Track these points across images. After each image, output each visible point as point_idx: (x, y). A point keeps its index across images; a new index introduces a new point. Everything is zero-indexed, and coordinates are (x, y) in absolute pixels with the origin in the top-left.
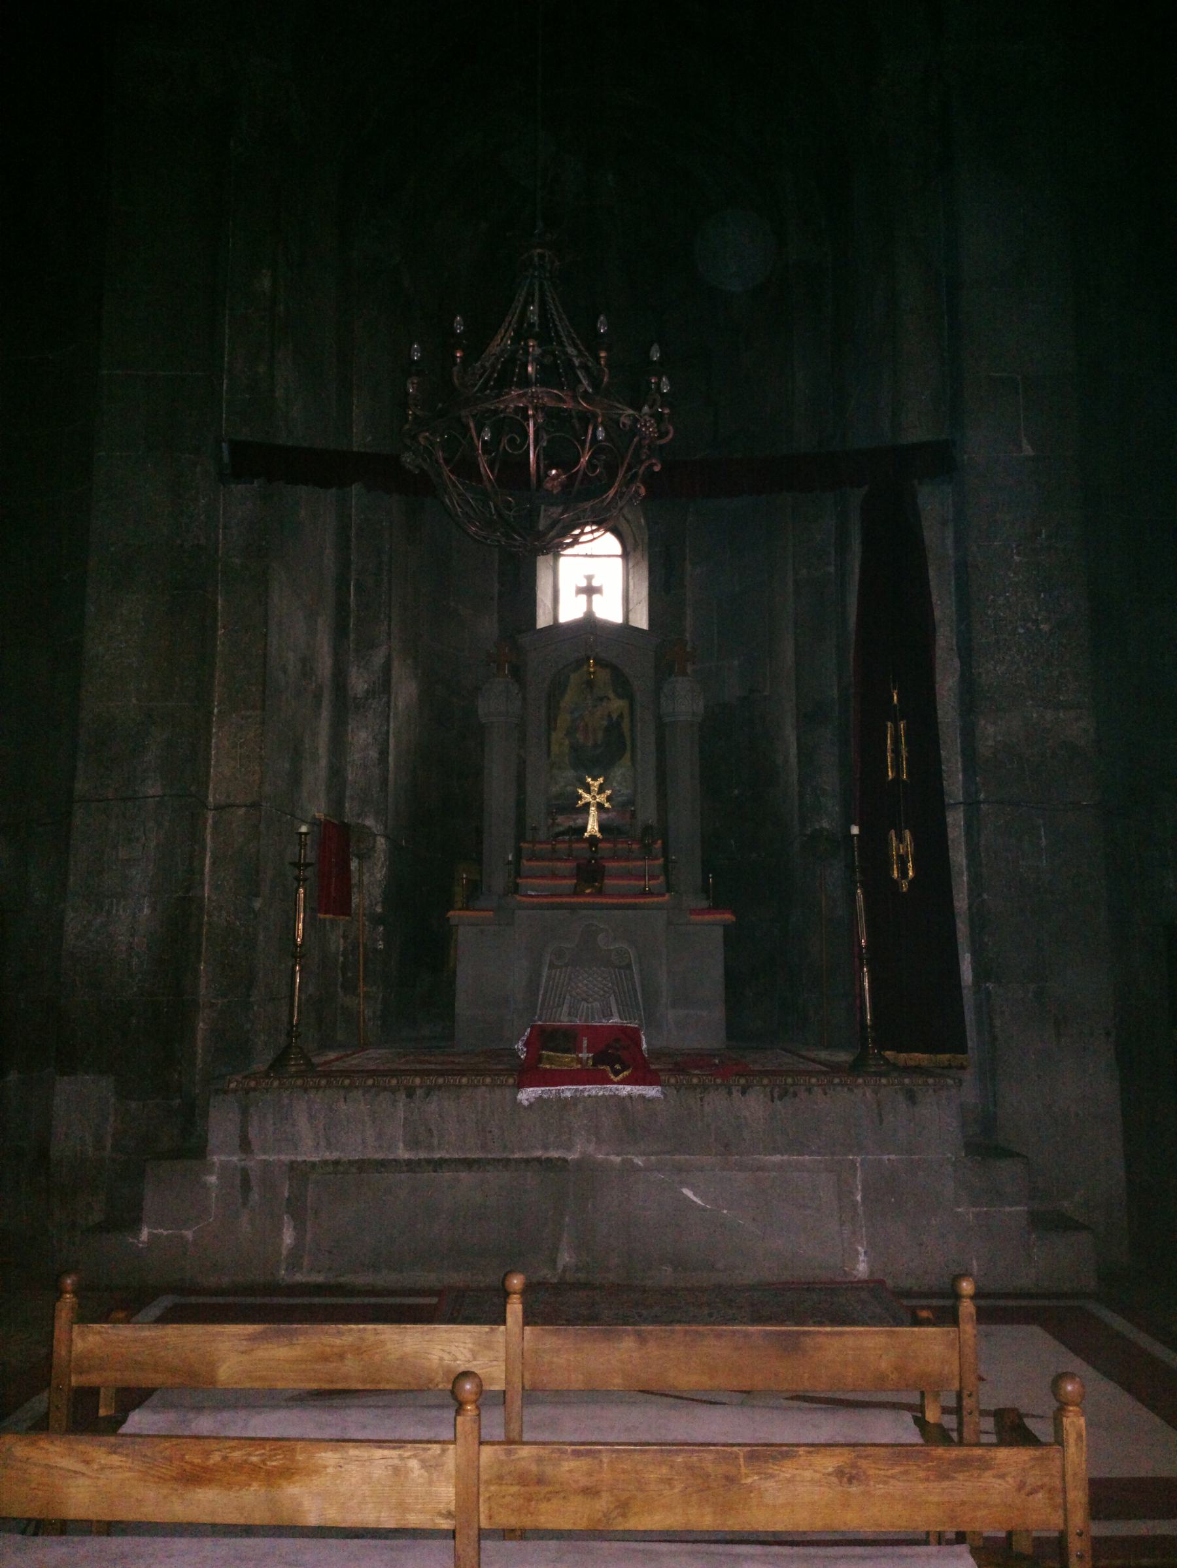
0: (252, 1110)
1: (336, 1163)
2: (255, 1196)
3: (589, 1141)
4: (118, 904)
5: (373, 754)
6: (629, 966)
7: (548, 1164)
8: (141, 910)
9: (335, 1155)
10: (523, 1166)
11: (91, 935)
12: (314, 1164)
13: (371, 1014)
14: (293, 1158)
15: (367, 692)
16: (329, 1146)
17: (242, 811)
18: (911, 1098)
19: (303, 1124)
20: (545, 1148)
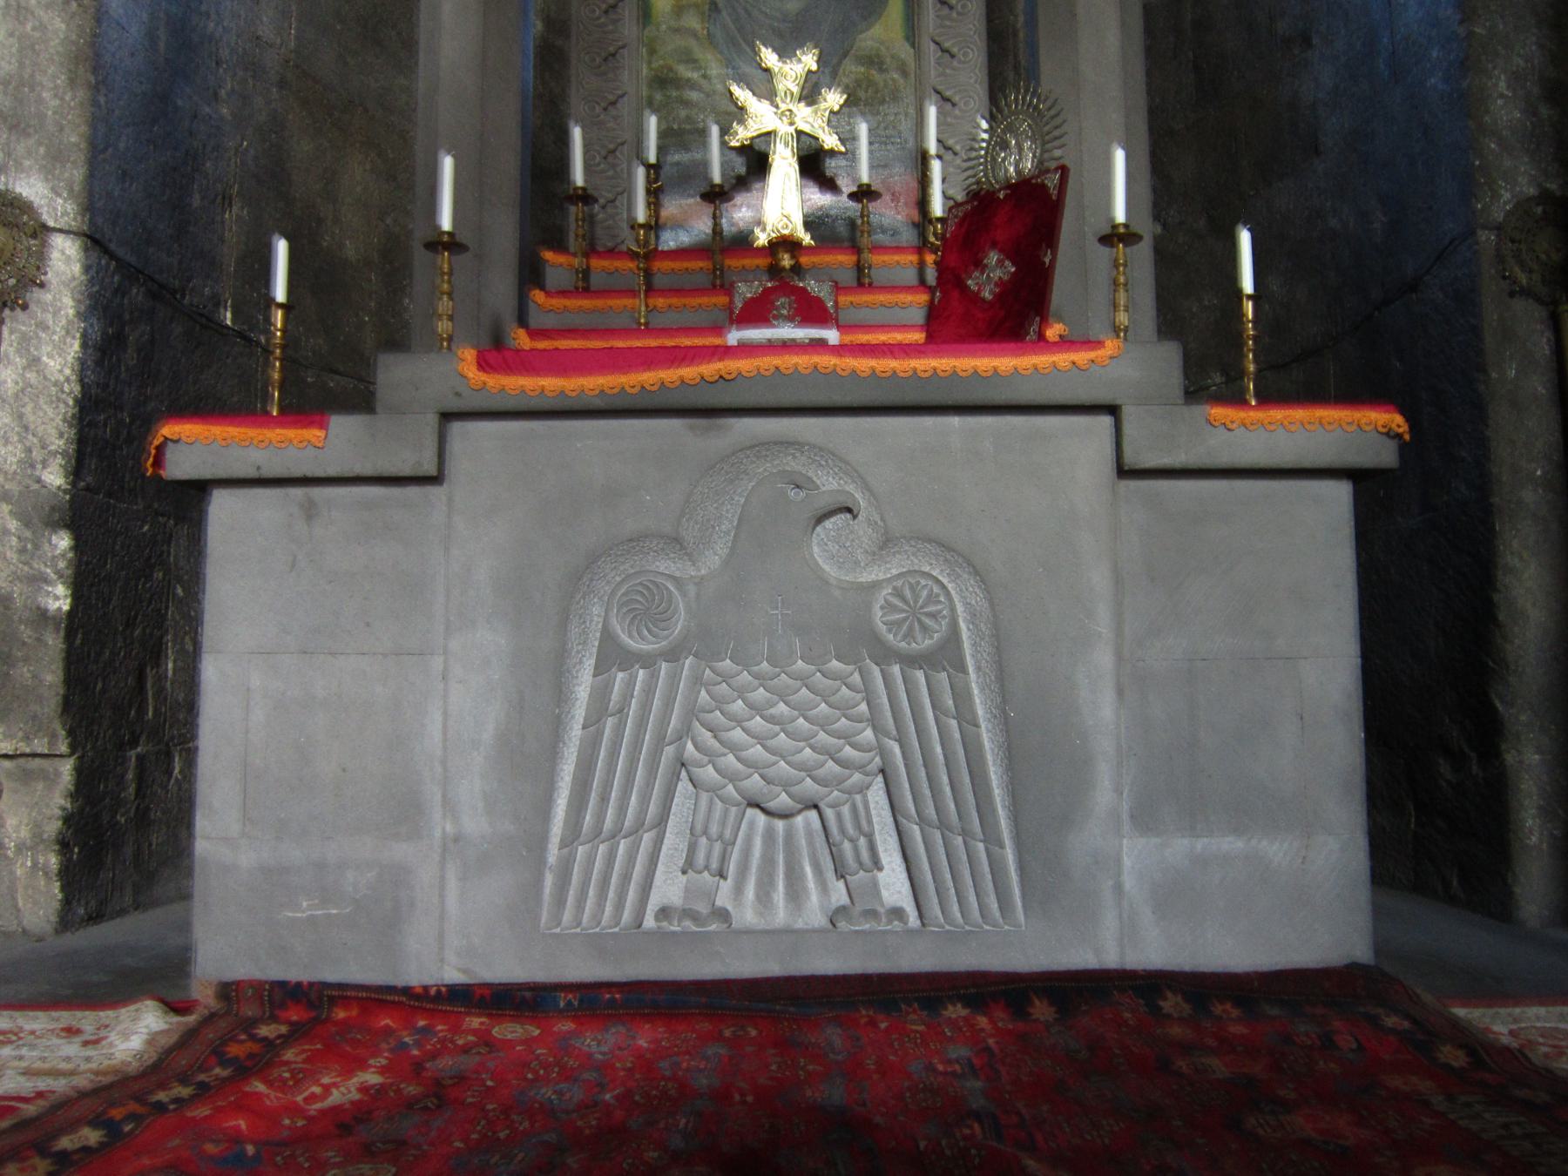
6: (946, 656)
13: (25, 833)
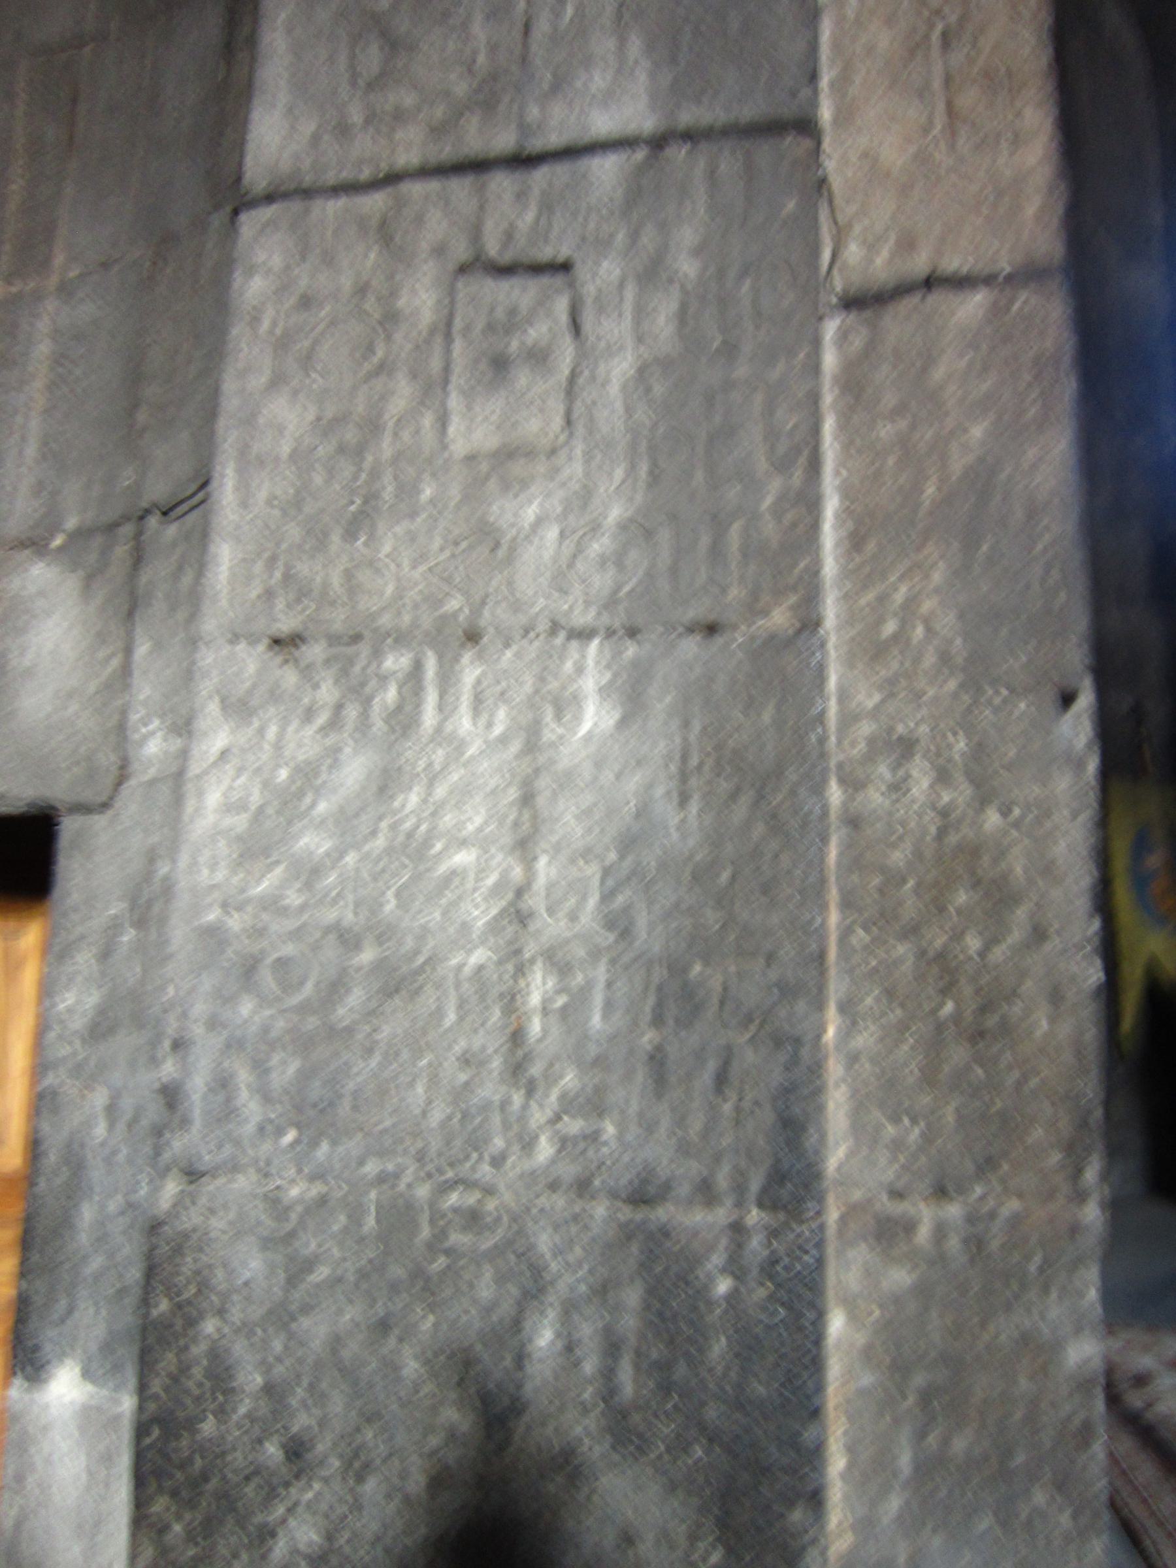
4: (446, 680)
8: (565, 705)
11: (312, 842)
17: (973, 305)
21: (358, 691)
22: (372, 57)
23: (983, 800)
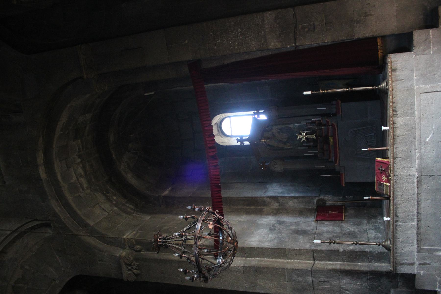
0: (402, 262)
1: (418, 241)
2: (427, 262)
3: (412, 170)
5: (295, 200)
7: (419, 182)
8: (344, 282)
9: (416, 241)
10: (419, 189)
12: (418, 247)
14: (416, 252)
15: (277, 202)
16: (412, 243)
17: (315, 254)
18: (394, 70)
19: (406, 249)
20: (414, 183)
21: (343, 292)
22: (306, 290)
23: (345, 255)
